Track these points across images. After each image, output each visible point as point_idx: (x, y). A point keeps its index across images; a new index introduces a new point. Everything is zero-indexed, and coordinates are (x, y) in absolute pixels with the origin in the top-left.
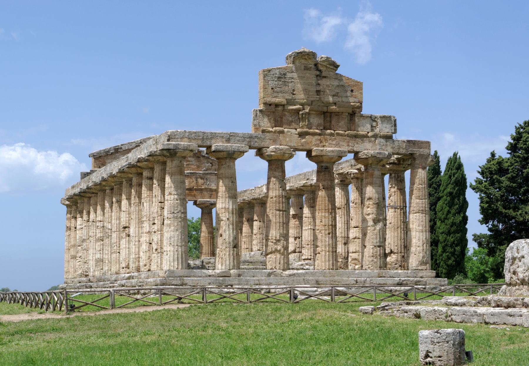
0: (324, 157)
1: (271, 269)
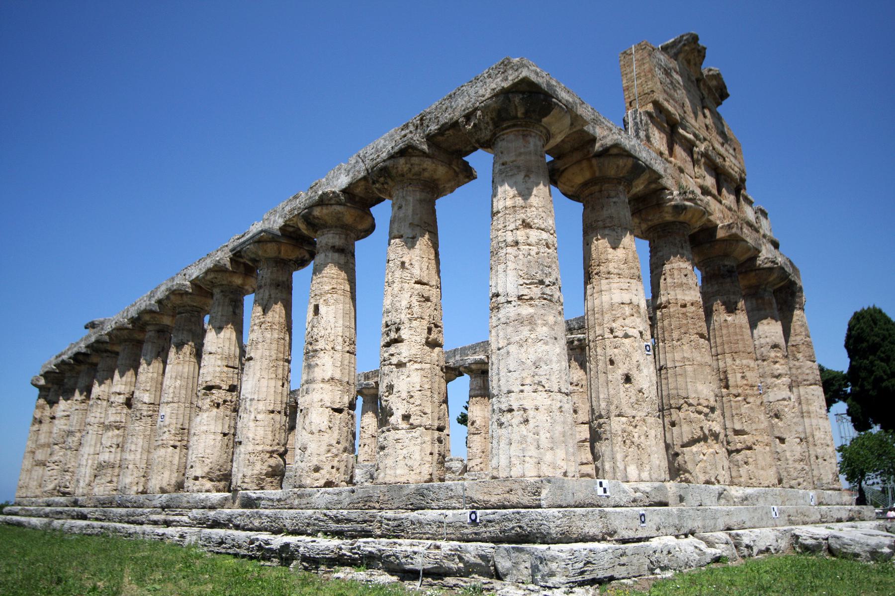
0: (741, 244)
1: (708, 482)
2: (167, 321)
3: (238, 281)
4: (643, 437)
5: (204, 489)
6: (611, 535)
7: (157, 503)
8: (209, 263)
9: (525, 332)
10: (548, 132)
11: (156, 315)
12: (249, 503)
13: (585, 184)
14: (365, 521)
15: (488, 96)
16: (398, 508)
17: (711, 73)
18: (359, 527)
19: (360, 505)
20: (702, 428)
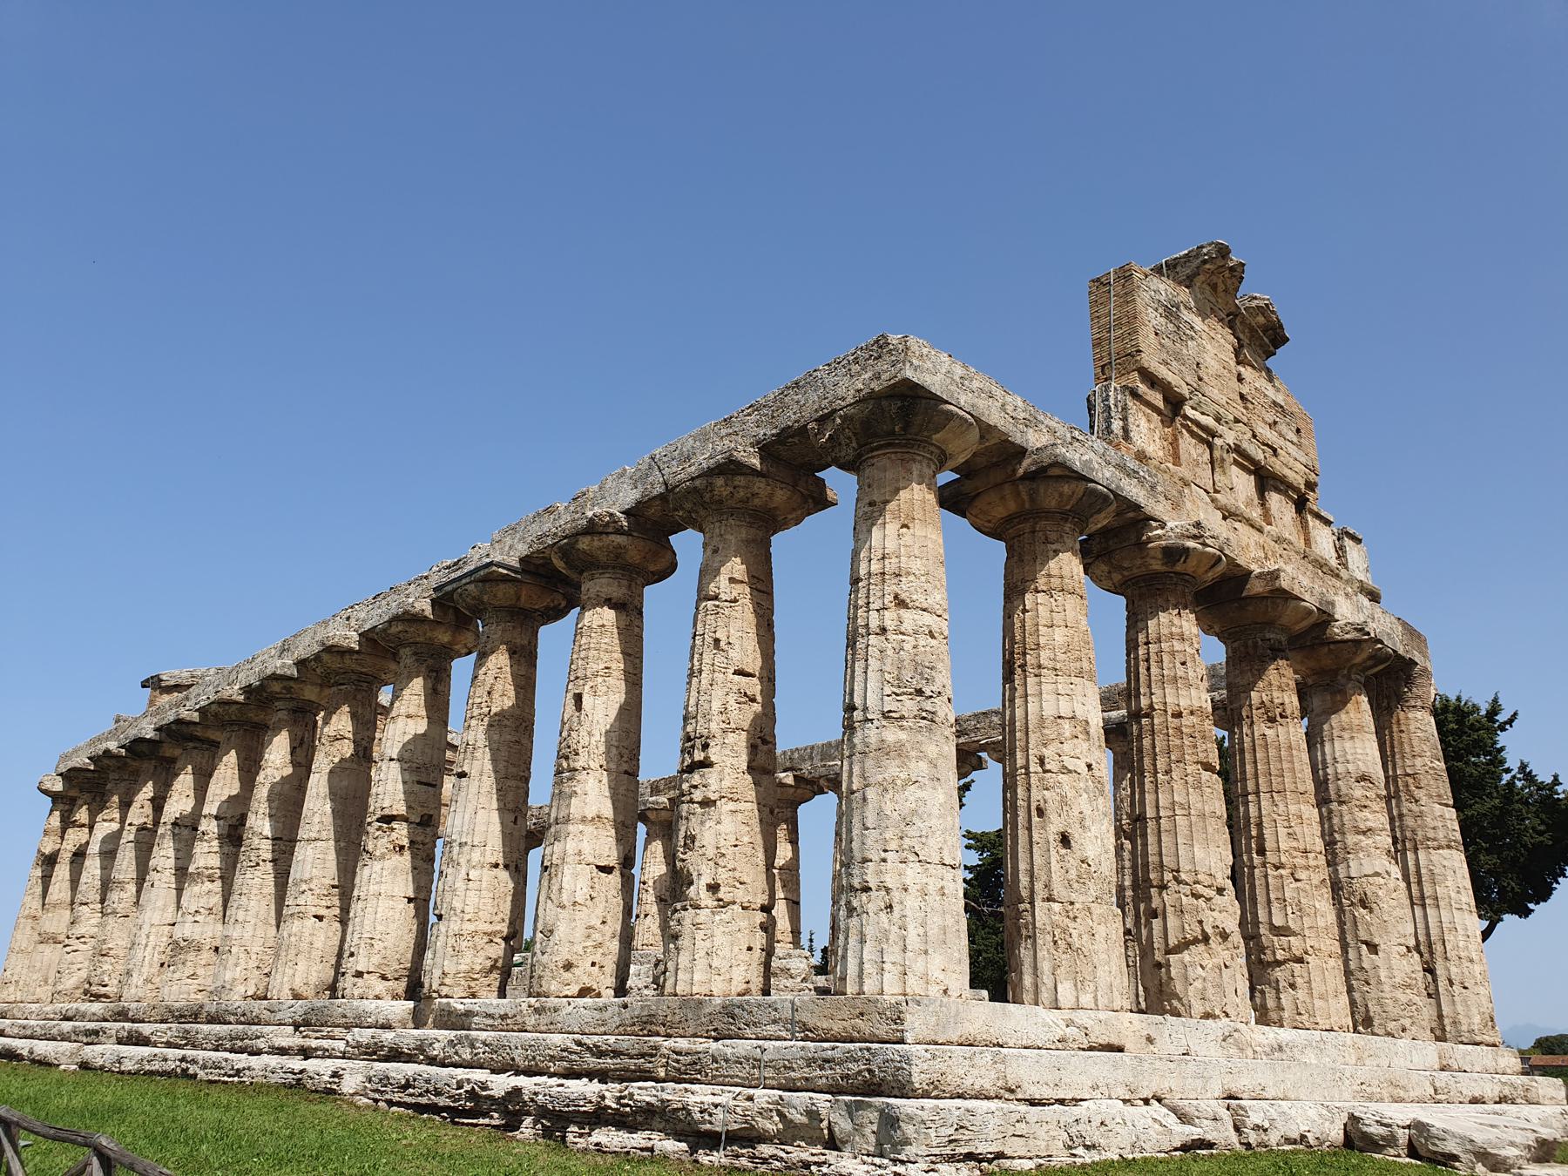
0: (1293, 603)
1: (1207, 1016)
2: (310, 693)
3: (444, 637)
4: (1085, 937)
5: (371, 994)
6: (1012, 1091)
7: (285, 1015)
8: (392, 606)
9: (892, 769)
10: (943, 452)
11: (292, 684)
12: (456, 1021)
13: (1009, 519)
14: (643, 1055)
15: (850, 400)
16: (695, 1036)
17: (1254, 303)
18: (632, 1063)
19: (636, 1028)
20: (1200, 922)
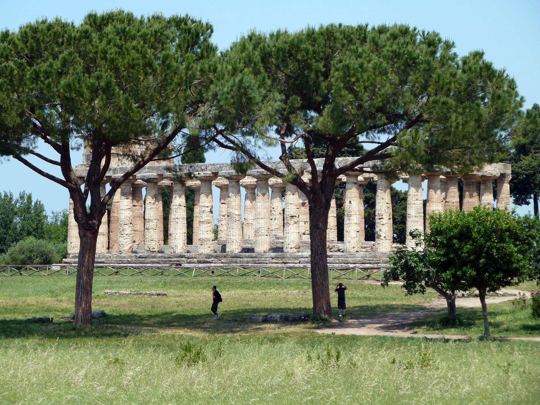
9: (416, 224)
